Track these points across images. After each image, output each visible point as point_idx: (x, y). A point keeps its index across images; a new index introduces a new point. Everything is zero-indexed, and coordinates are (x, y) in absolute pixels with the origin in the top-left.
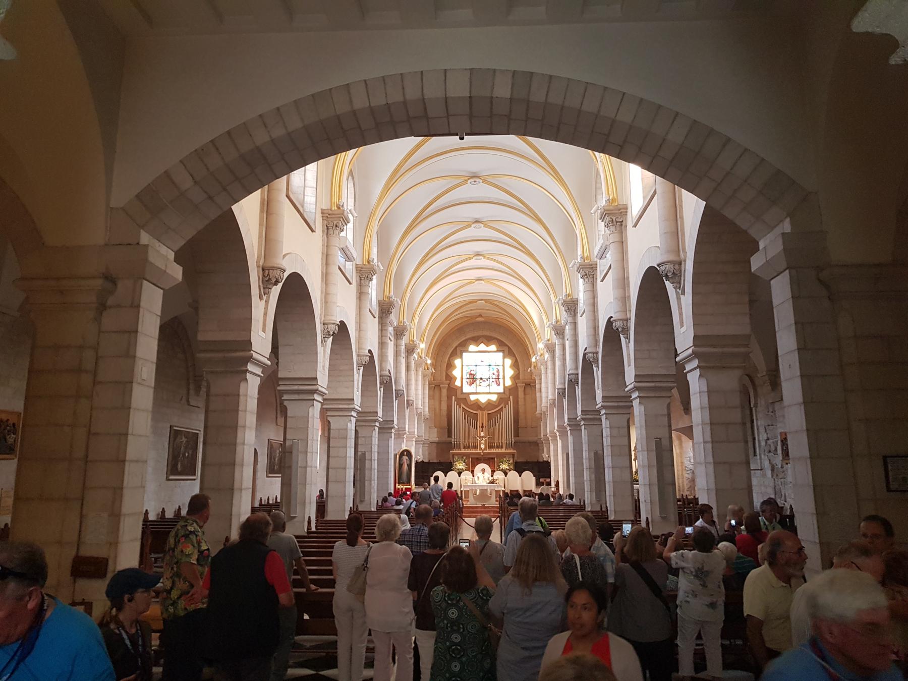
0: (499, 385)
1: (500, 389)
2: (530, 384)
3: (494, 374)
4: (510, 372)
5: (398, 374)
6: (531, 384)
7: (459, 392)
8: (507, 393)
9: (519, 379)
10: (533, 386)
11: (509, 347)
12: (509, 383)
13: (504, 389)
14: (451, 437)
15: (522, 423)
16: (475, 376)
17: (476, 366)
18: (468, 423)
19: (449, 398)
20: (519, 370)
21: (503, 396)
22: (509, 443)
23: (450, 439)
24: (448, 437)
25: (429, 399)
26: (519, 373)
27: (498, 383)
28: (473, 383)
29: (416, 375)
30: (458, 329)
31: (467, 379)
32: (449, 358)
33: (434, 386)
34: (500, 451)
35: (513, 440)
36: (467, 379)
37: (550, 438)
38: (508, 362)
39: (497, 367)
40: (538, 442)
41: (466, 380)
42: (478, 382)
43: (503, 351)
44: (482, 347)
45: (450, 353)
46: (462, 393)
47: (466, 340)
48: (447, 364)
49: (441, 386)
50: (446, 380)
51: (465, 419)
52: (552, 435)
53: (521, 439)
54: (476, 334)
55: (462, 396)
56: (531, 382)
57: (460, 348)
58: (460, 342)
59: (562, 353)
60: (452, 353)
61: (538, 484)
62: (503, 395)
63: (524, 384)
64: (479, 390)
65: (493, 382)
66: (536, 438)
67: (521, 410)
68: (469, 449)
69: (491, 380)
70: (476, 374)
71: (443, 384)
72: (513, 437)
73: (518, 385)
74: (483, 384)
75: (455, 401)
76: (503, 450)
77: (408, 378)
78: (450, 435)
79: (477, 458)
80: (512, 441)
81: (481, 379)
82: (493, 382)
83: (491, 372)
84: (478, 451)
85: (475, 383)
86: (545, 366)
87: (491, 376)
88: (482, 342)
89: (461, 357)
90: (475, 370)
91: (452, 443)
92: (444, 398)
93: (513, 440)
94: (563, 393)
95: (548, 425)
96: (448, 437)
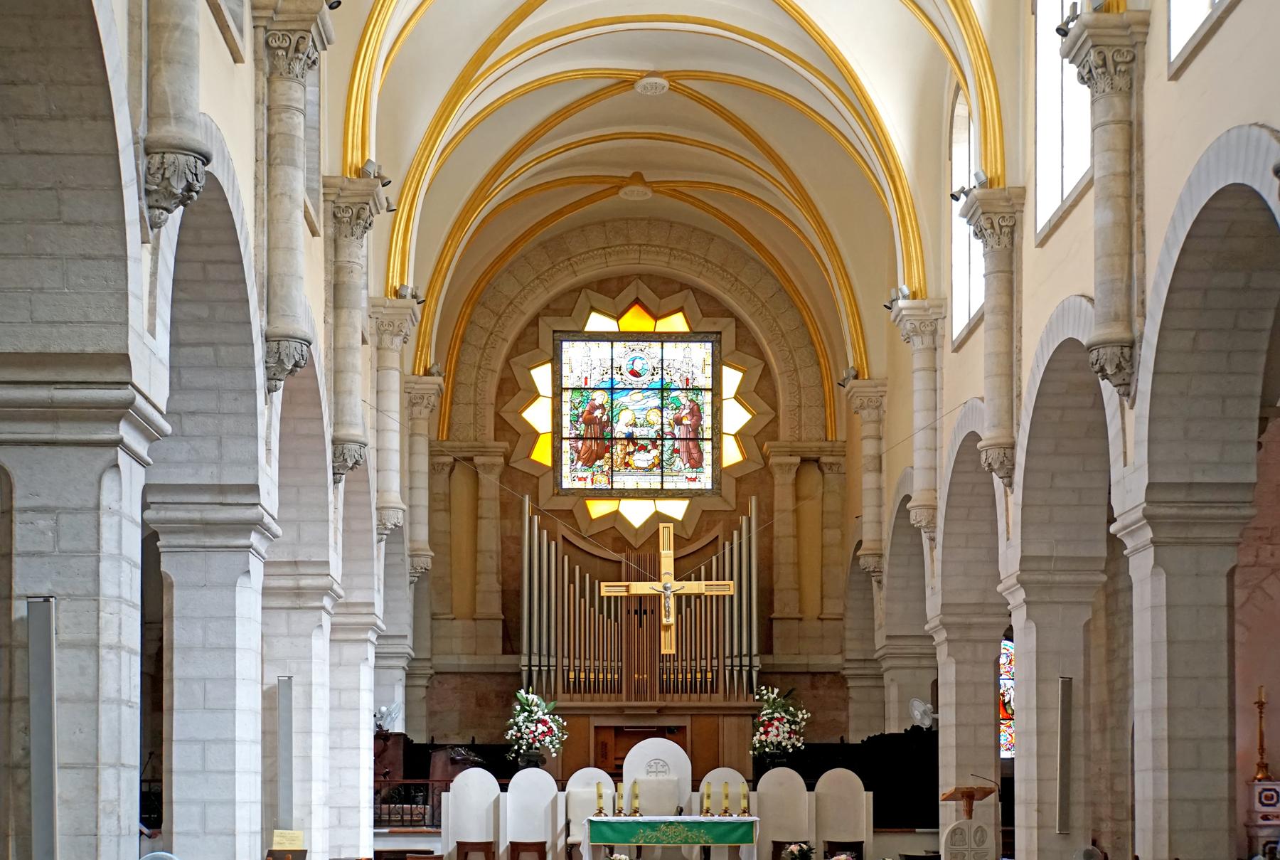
0: (696, 464)
1: (705, 481)
2: (817, 461)
3: (678, 421)
4: (736, 417)
5: (280, 256)
6: (824, 459)
7: (546, 487)
8: (729, 489)
9: (776, 438)
10: (831, 464)
11: (739, 323)
12: (732, 454)
13: (716, 479)
14: (517, 652)
15: (784, 605)
16: (609, 428)
17: (612, 390)
18: (582, 595)
19: (509, 509)
20: (775, 407)
21: (715, 504)
22: (741, 666)
23: (510, 659)
24: (505, 652)
25: (432, 511)
26: (775, 420)
27: (695, 455)
28: (601, 458)
29: (380, 368)
30: (543, 245)
31: (578, 438)
32: (508, 361)
33: (449, 459)
34: (705, 701)
35: (756, 661)
36: (578, 438)
37: (941, 636)
38: (732, 379)
39: (691, 395)
40: (844, 672)
41: (572, 442)
42: (618, 450)
43: (713, 337)
44: (636, 321)
45: (511, 339)
46: (559, 491)
47: (576, 291)
48: (502, 381)
49: (478, 460)
50: (495, 440)
51: (572, 581)
52: (950, 619)
53: (781, 657)
54: (616, 265)
55: (564, 504)
56: (821, 450)
57: (549, 319)
58: (554, 292)
59: (1120, 168)
60: (521, 337)
61: (885, 820)
62: (716, 499)
63: (797, 460)
64: (624, 481)
65: (676, 451)
66: (837, 660)
67: (784, 551)
68: (588, 696)
69: (668, 443)
70: (611, 421)
71: (483, 454)
72: (755, 651)
73: (773, 460)
74: (642, 459)
75: (533, 513)
76: (718, 700)
77: (341, 343)
78: (511, 642)
79: (618, 731)
80: (751, 666)
81: (630, 438)
82: (676, 451)
83: (669, 415)
84: (624, 703)
85: (608, 455)
86: (928, 340)
87: (667, 429)
88: (637, 301)
89: (556, 360)
90: (607, 406)
91: (519, 674)
92: (490, 509)
93: (756, 661)
94: (1119, 367)
95: (934, 581)
96: (505, 652)
